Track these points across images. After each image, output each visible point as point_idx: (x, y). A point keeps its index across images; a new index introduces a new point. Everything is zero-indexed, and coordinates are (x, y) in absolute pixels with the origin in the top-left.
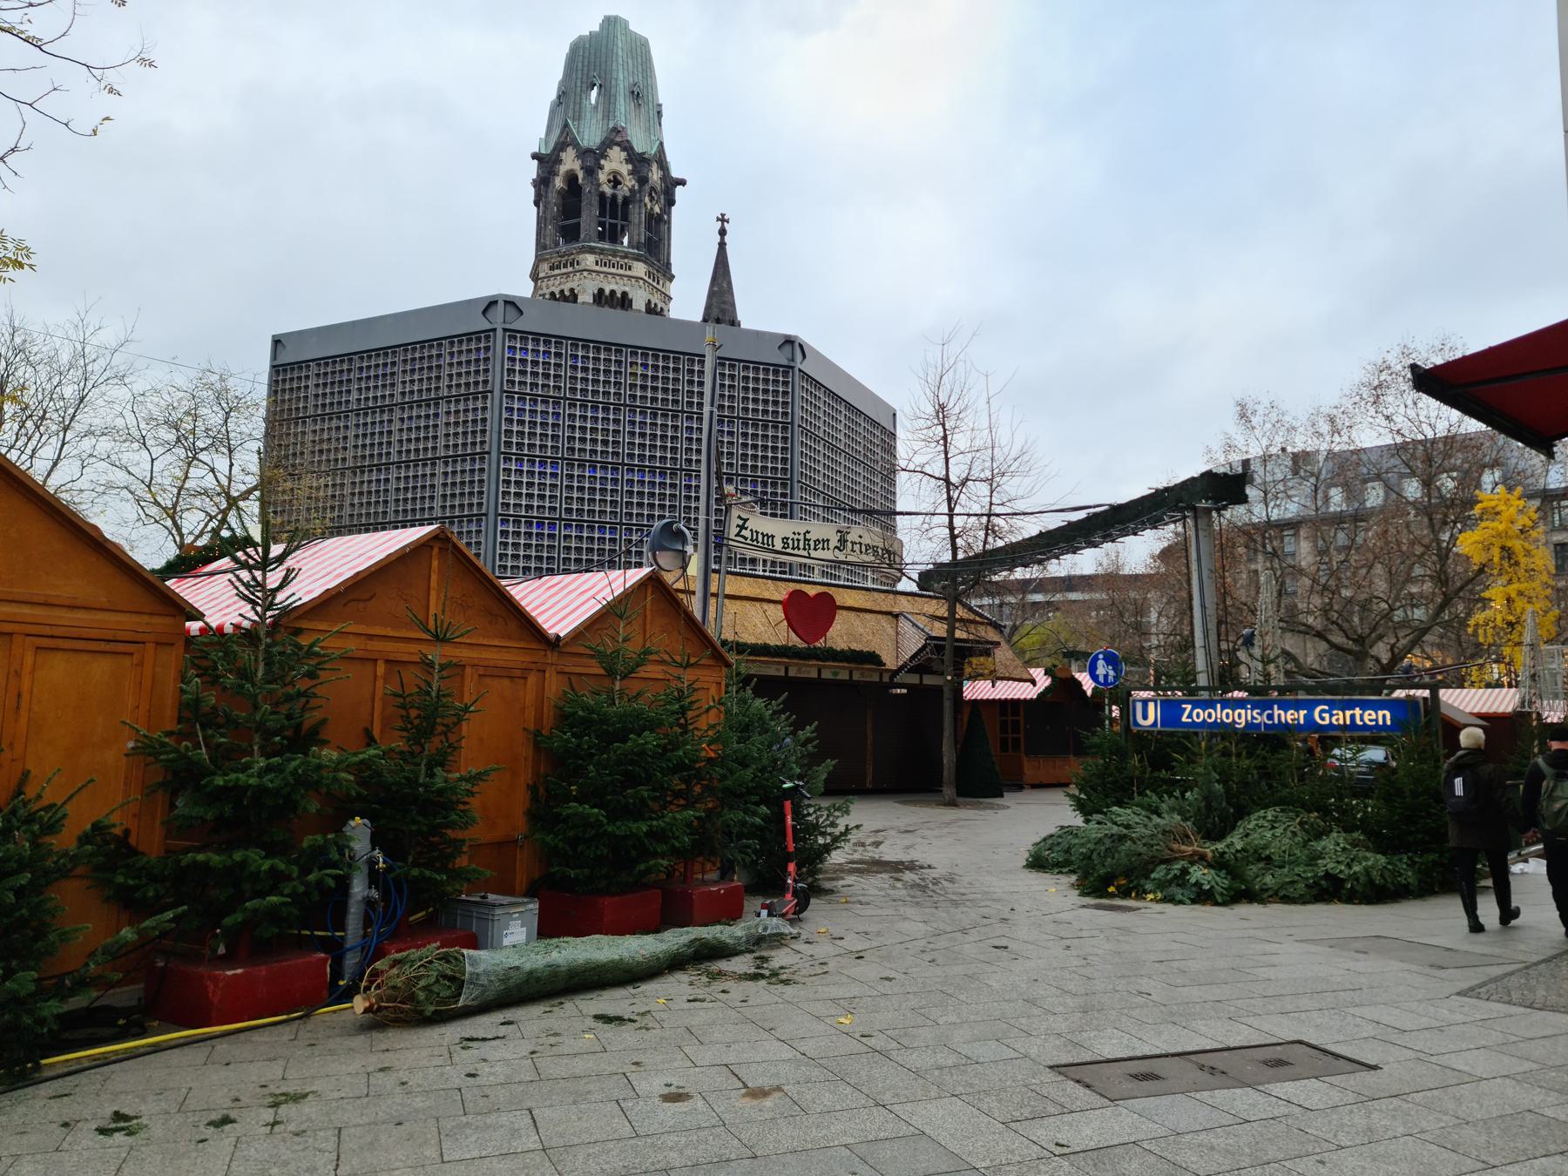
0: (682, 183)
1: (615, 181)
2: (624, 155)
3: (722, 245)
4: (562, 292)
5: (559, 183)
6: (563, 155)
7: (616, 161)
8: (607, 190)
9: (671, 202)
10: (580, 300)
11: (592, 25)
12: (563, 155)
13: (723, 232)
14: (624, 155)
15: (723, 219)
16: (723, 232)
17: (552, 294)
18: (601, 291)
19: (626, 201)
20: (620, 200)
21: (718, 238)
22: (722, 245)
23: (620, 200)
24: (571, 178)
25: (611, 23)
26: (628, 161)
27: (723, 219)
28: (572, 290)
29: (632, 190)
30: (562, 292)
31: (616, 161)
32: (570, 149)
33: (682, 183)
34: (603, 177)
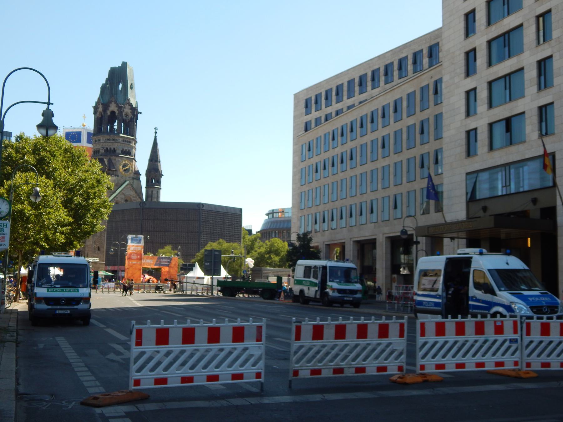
0: (141, 113)
1: (126, 115)
2: (129, 107)
3: (156, 137)
4: (111, 149)
5: (109, 113)
6: (111, 105)
7: (127, 110)
8: (124, 117)
9: (137, 119)
10: (117, 151)
11: (118, 64)
12: (111, 105)
13: (156, 133)
14: (129, 107)
15: (156, 129)
16: (156, 133)
17: (107, 149)
18: (123, 149)
19: (130, 121)
20: (127, 121)
21: (154, 134)
22: (156, 137)
23: (127, 121)
24: (113, 113)
25: (124, 64)
26: (130, 109)
27: (156, 129)
28: (114, 149)
29: (131, 118)
30: (111, 149)
31: (127, 110)
32: (113, 103)
33: (141, 113)
34: (124, 114)
